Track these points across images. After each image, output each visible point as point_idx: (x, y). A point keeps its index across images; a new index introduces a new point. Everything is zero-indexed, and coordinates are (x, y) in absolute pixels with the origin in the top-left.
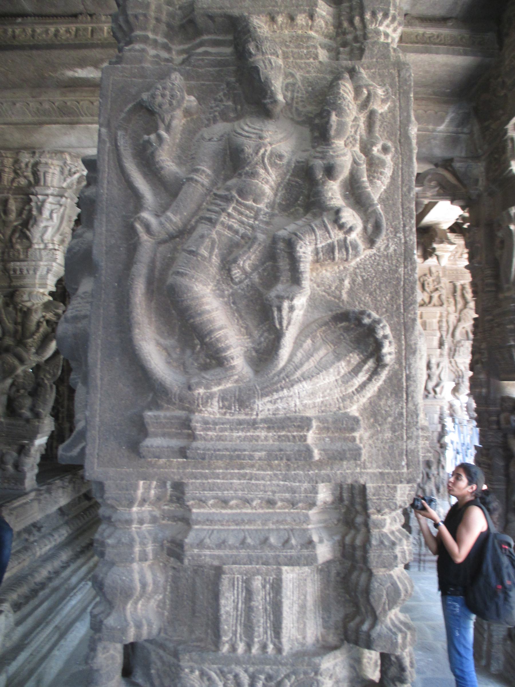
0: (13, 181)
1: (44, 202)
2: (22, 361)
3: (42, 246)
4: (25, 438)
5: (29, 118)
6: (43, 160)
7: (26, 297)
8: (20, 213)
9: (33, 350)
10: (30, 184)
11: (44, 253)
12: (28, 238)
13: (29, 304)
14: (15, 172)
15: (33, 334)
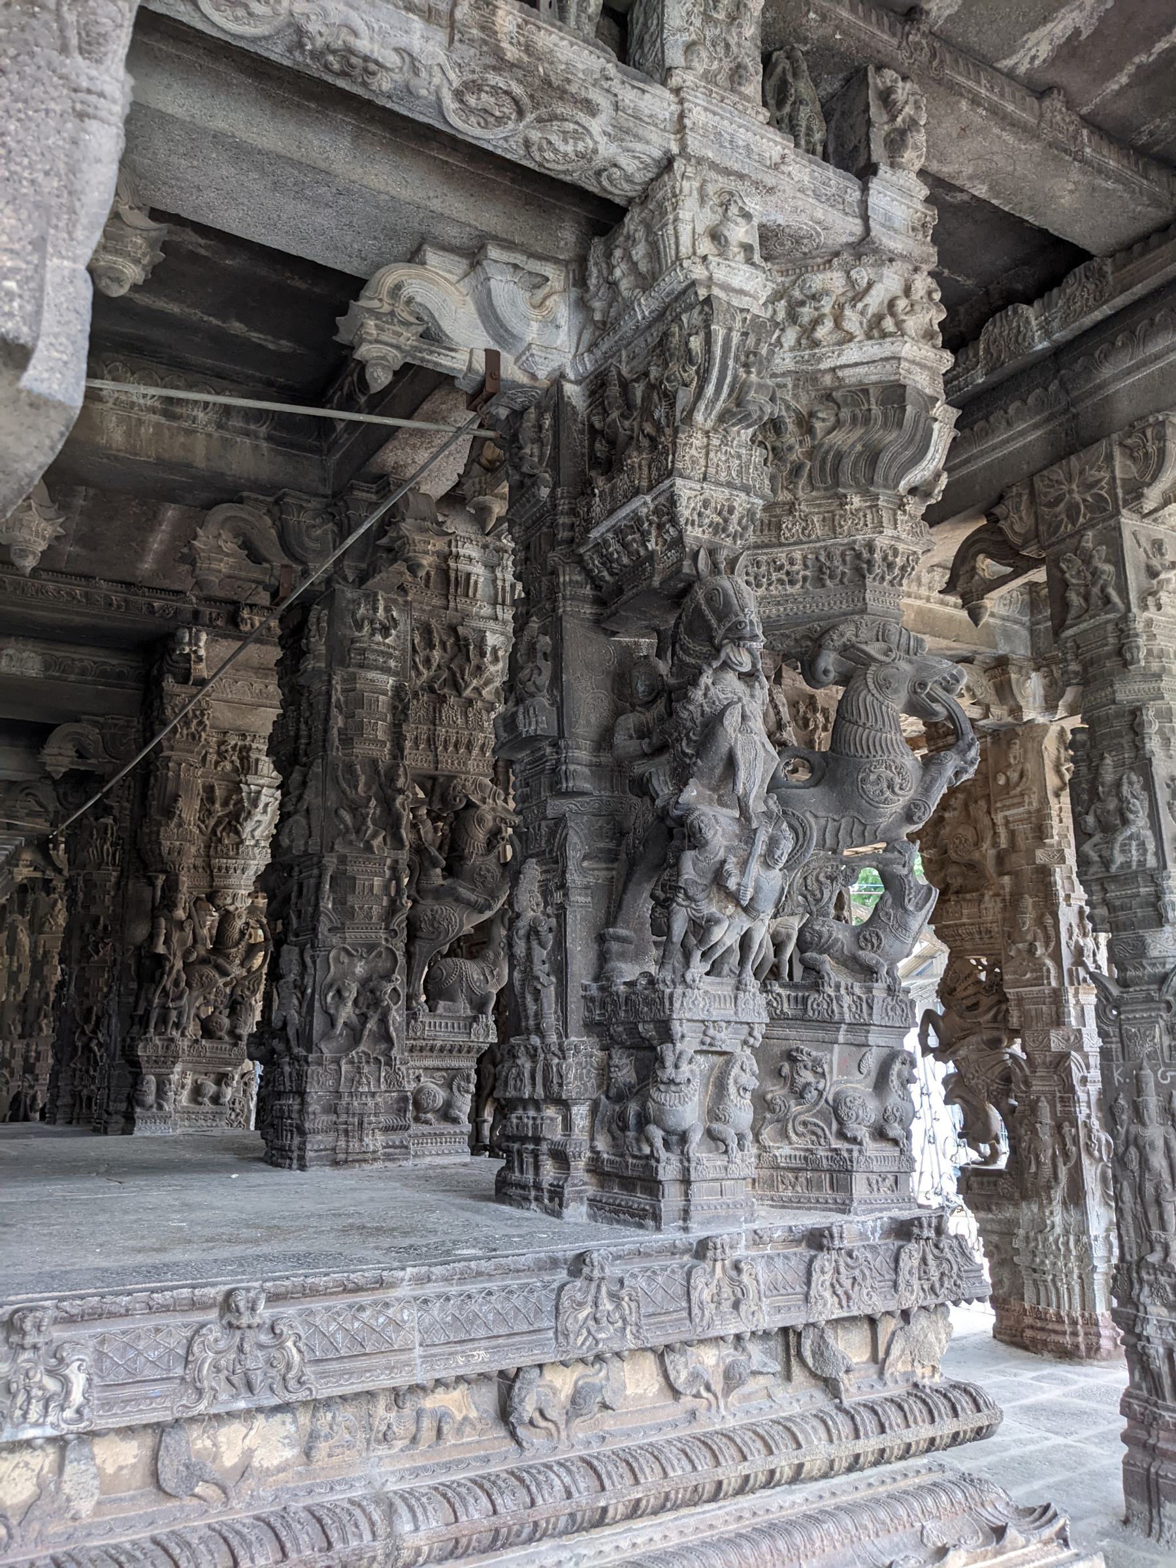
0: (217, 763)
1: (259, 792)
2: (224, 973)
3: (253, 842)
4: (228, 1064)
5: (248, 699)
6: (254, 746)
7: (229, 900)
8: (225, 804)
9: (237, 961)
10: (236, 770)
11: (257, 851)
12: (238, 833)
13: (231, 908)
14: (219, 753)
15: (238, 943)
